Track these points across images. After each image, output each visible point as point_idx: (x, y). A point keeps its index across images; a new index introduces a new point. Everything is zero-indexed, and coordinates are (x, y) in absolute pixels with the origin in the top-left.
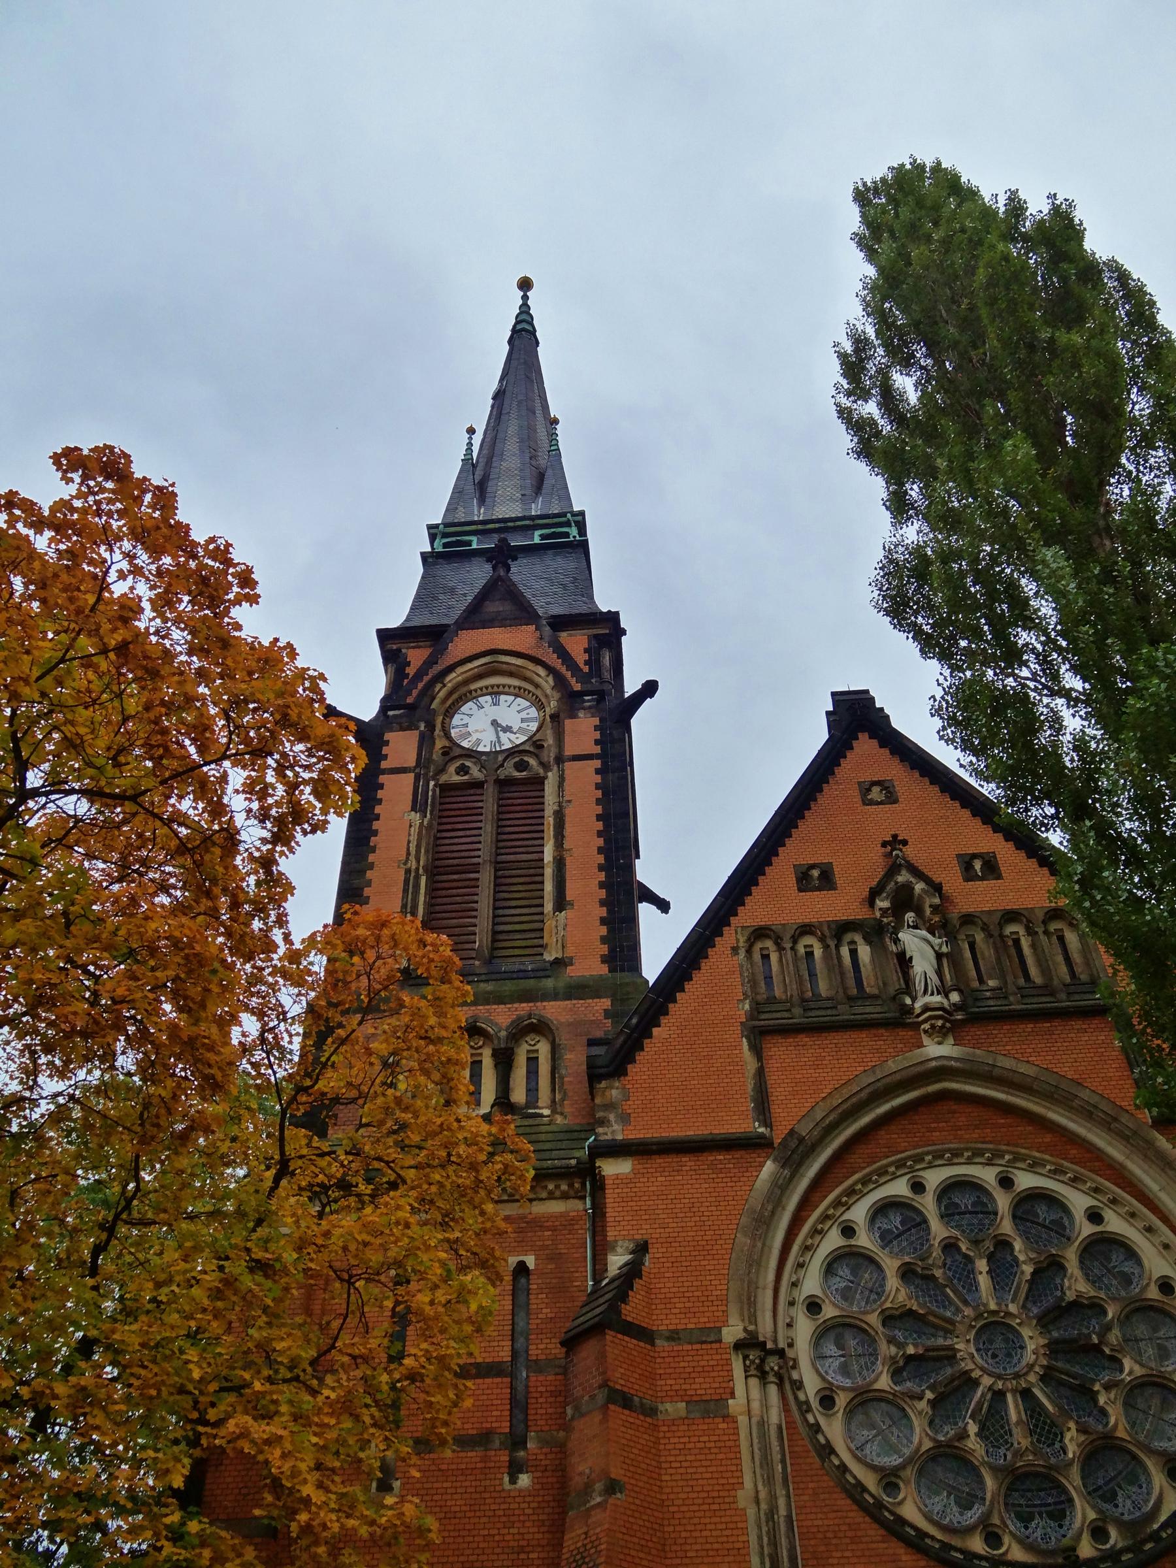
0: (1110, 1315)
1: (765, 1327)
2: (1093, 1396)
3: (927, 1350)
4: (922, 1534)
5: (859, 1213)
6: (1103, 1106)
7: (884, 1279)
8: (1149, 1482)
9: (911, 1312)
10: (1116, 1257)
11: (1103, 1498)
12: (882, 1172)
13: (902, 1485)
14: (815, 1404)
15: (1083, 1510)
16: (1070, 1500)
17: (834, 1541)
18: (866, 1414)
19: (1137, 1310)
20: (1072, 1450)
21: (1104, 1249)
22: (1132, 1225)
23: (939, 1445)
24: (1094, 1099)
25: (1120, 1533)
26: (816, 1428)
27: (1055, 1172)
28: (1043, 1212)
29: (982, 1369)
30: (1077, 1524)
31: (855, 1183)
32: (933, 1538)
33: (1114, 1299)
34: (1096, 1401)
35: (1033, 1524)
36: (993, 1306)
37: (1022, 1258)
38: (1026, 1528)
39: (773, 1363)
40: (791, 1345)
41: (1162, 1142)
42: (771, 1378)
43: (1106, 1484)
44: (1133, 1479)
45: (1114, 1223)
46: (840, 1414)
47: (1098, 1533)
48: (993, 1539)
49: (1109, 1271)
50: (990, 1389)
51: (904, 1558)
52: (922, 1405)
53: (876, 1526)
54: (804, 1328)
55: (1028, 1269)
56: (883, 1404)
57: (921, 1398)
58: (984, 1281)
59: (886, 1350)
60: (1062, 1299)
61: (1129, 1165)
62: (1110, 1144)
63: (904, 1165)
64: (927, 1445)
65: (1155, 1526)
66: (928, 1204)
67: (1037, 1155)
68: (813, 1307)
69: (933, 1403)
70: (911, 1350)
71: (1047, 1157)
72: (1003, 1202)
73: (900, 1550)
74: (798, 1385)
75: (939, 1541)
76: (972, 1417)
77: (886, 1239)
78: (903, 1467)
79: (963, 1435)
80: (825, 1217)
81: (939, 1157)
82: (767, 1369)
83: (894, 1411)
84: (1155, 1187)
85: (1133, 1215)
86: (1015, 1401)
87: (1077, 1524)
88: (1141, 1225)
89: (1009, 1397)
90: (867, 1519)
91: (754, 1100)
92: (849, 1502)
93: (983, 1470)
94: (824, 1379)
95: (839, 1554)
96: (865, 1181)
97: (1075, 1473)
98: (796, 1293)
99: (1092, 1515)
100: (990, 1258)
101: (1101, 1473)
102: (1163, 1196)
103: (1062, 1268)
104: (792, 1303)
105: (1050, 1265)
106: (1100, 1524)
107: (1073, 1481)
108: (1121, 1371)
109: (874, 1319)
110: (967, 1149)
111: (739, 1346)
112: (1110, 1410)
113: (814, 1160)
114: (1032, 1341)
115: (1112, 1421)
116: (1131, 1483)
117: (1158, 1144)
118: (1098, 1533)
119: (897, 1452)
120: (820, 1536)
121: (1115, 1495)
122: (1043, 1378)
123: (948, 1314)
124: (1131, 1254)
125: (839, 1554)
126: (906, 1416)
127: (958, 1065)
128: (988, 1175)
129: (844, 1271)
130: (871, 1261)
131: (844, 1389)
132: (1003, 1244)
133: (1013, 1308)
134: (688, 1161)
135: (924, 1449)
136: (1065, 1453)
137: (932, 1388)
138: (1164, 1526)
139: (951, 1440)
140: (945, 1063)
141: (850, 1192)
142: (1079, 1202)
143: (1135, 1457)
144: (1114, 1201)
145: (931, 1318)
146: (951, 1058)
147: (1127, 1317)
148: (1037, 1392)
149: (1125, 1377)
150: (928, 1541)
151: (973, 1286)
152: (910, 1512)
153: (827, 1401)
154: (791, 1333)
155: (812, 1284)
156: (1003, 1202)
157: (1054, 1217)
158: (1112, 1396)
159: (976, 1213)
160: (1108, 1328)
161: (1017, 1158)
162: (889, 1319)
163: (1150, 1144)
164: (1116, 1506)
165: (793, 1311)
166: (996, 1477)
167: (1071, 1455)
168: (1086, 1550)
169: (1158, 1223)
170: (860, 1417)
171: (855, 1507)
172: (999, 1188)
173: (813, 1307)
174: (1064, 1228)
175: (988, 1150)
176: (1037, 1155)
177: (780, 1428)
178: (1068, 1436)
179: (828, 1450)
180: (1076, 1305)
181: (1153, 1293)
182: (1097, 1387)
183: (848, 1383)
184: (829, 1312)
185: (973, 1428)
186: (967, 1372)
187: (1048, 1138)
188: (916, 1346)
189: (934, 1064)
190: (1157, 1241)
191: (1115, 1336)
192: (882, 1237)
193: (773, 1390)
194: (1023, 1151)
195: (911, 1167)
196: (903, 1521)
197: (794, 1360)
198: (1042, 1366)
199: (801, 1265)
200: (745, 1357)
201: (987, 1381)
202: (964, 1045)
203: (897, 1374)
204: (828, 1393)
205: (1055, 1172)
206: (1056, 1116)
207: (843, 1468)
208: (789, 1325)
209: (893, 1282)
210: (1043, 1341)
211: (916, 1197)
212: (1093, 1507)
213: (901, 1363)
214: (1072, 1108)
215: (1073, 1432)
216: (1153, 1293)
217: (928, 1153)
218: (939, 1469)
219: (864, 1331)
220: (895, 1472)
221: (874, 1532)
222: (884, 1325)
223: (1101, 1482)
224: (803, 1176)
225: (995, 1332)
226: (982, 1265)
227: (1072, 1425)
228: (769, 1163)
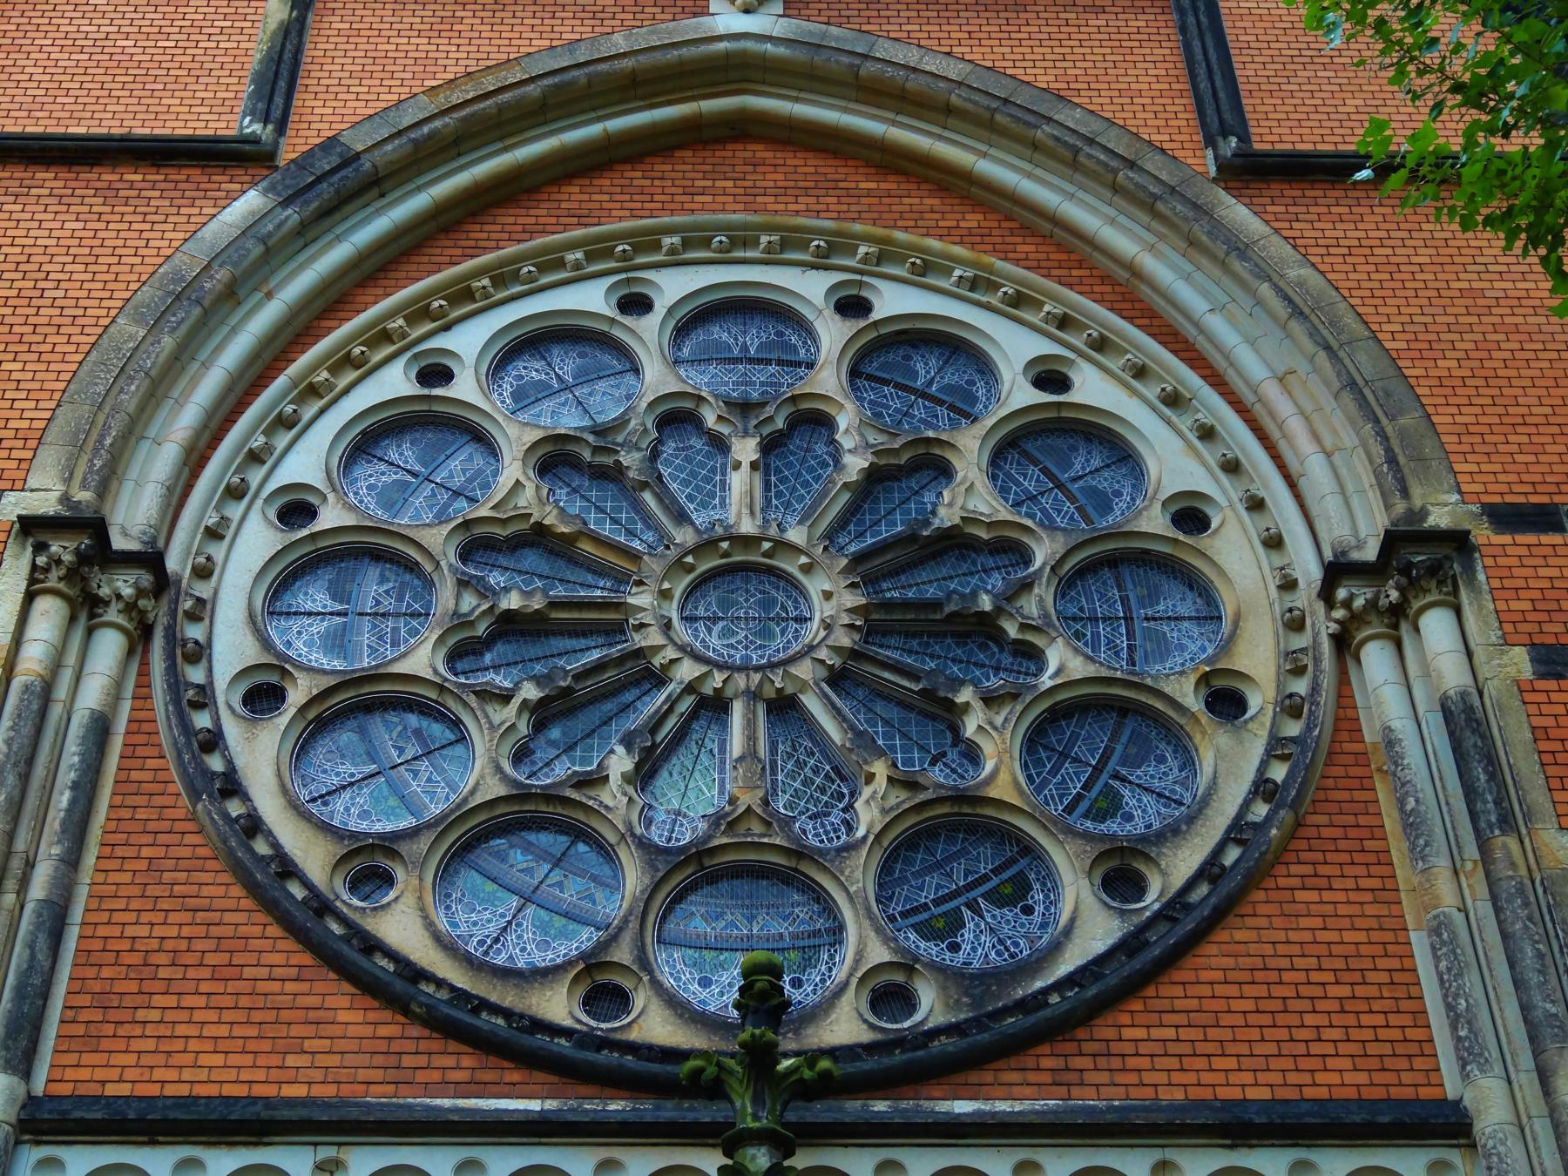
0: (1038, 563)
1: (132, 517)
2: (950, 715)
3: (554, 605)
4: (414, 974)
5: (469, 341)
6: (1112, 140)
7: (496, 473)
8: (1051, 904)
9: (541, 530)
10: (1085, 461)
11: (927, 931)
12: (550, 261)
13: (400, 873)
14: (227, 695)
15: (861, 941)
16: (838, 930)
17: (162, 973)
18: (363, 732)
19: (1112, 561)
20: (868, 817)
21: (1057, 438)
22: (1134, 392)
23: (523, 795)
24: (1089, 127)
25: (943, 989)
26: (213, 741)
27: (974, 284)
28: (925, 369)
29: (682, 648)
30: (840, 974)
31: (478, 273)
32: (440, 983)
33: (1051, 527)
34: (955, 730)
35: (725, 978)
36: (747, 527)
37: (847, 442)
38: (705, 983)
39: (125, 583)
40: (203, 572)
41: (1237, 212)
42: (113, 614)
43: (938, 902)
44: (1015, 894)
45: (1092, 388)
46: (284, 720)
47: (890, 997)
48: (605, 996)
49: (1060, 486)
50: (690, 688)
51: (343, 1016)
52: (509, 713)
53: (290, 944)
54: (256, 542)
55: (855, 465)
56: (413, 720)
57: (505, 698)
58: (739, 481)
59: (445, 596)
60: (927, 523)
61: (1151, 264)
62: (1112, 222)
63: (608, 253)
64: (495, 789)
65: (1039, 984)
66: (648, 334)
67: (935, 244)
68: (296, 509)
69: (543, 714)
70: (513, 601)
71: (958, 250)
72: (833, 334)
73: (340, 1000)
74: (200, 653)
75: (452, 988)
76: (628, 741)
77: (524, 398)
78: (412, 833)
79: (596, 780)
80: (380, 336)
81: (694, 244)
82: (105, 591)
83: (439, 731)
84: (1196, 303)
85: (1140, 372)
86: (750, 724)
87: (840, 974)
88: (1152, 392)
89: (738, 709)
90: (274, 930)
91: (258, 78)
92: (237, 891)
93: (623, 853)
94: (266, 644)
95: (171, 1001)
96: (499, 281)
97: (861, 873)
98: (255, 476)
99: (879, 954)
100: (771, 446)
101: (933, 880)
102: (1217, 324)
103: (944, 471)
104: (235, 493)
105: (915, 467)
106: (899, 978)
107: (855, 881)
108: (1041, 669)
109: (439, 540)
110: (769, 228)
111: (30, 526)
112: (988, 747)
113: (379, 212)
114: (830, 601)
115: (989, 766)
116: (998, 899)
117: (1220, 212)
118: (890, 997)
119: (408, 803)
120: (135, 959)
121: (956, 923)
122: (837, 679)
123: (636, 544)
124: (1120, 453)
125: (171, 1001)
126: (462, 738)
127: (781, 51)
128: (809, 288)
129: (404, 453)
130: (481, 438)
131: (310, 670)
132: (813, 421)
133: (796, 535)
134: (48, 180)
135: (479, 799)
136: (850, 828)
137: (538, 680)
138: (1058, 986)
139: (561, 784)
140: (750, 45)
141: (461, 293)
142: (1013, 346)
143: (1028, 849)
144: (1101, 344)
145: (586, 546)
146: (769, 38)
147: (1082, 572)
148: (812, 704)
149: (1046, 681)
150: (430, 989)
151: (713, 491)
152: (400, 926)
153: (262, 697)
154: (217, 551)
155: (306, 461)
156: (833, 334)
157: (951, 377)
158: (999, 720)
159: (768, 362)
160: (1026, 586)
161: (887, 253)
162: (478, 545)
163: (1201, 210)
164: (954, 947)
165: (235, 511)
166: (651, 865)
167: (860, 833)
168: (845, 1026)
169: (1192, 380)
170: (346, 736)
171: (247, 903)
172: (829, 312)
173: (296, 509)
174: (974, 400)
175: (820, 232)
176: (935, 244)
177: (101, 727)
178: (867, 792)
179: (231, 786)
180: (956, 544)
181: (1155, 521)
182: (965, 695)
183: (327, 662)
184: (330, 517)
185: (620, 763)
186: (639, 653)
187: (972, 220)
188: (527, 595)
189: (722, 46)
190: (1184, 423)
191: (1030, 605)
192: (518, 395)
193: (109, 646)
194: (900, 235)
195: (625, 256)
196: (372, 945)
197: (200, 601)
198: (837, 650)
199: (284, 422)
200: (40, 548)
201: (687, 671)
202: (798, 16)
203: (462, 652)
204: (273, 678)
205: (974, 284)
206: (997, 168)
207: (253, 825)
208: (214, 534)
209: (512, 470)
210: (853, 599)
211: (627, 320)
212: (886, 940)
213: (481, 629)
214: (1035, 146)
215: (881, 783)
216: (1155, 521)
217: (670, 230)
218: (518, 857)
219: (412, 567)
220: (388, 845)
221: (284, 954)
222: (465, 554)
223: (926, 896)
224: (339, 239)
225: (739, 572)
226: (746, 450)
227: (880, 769)
228: (252, 193)
